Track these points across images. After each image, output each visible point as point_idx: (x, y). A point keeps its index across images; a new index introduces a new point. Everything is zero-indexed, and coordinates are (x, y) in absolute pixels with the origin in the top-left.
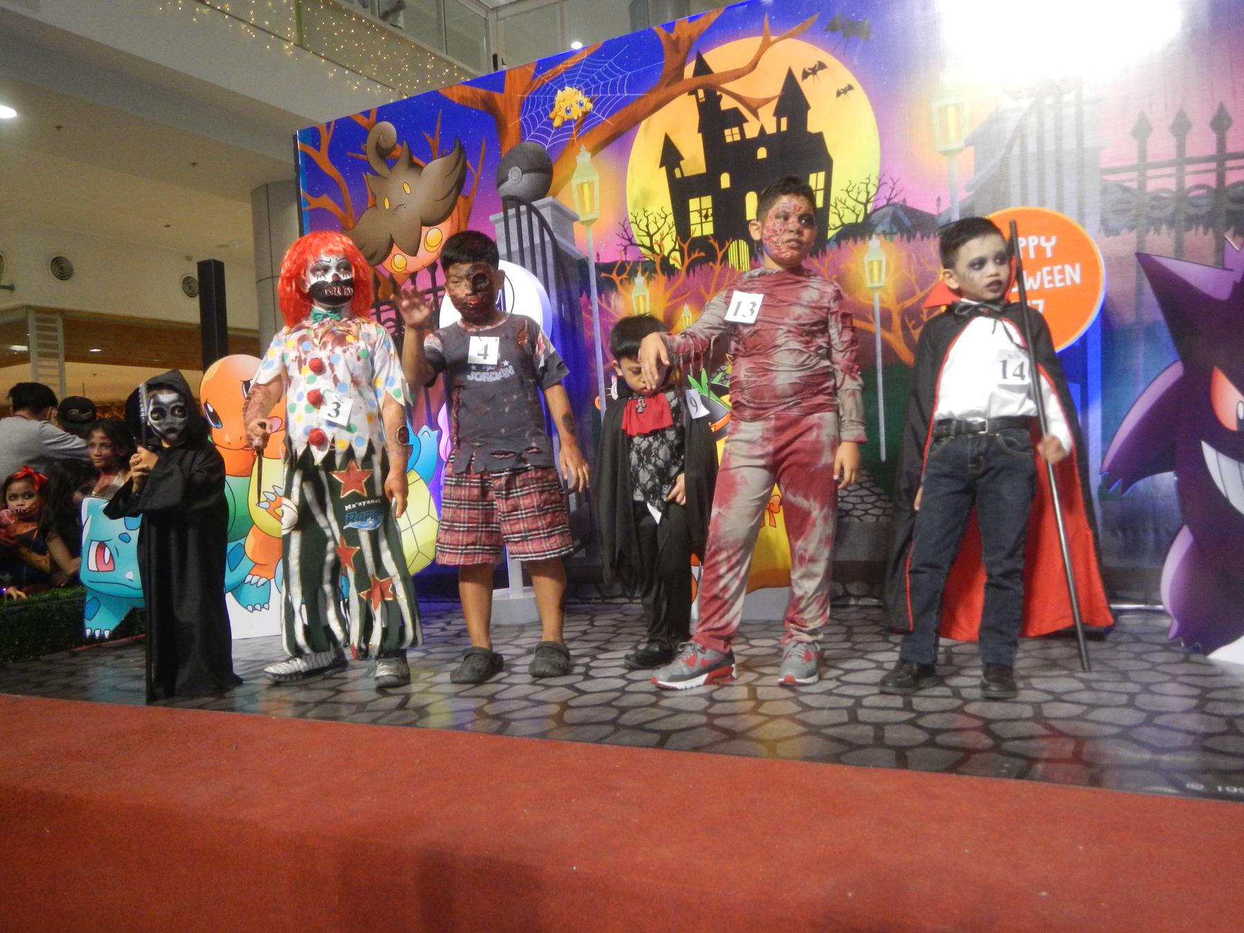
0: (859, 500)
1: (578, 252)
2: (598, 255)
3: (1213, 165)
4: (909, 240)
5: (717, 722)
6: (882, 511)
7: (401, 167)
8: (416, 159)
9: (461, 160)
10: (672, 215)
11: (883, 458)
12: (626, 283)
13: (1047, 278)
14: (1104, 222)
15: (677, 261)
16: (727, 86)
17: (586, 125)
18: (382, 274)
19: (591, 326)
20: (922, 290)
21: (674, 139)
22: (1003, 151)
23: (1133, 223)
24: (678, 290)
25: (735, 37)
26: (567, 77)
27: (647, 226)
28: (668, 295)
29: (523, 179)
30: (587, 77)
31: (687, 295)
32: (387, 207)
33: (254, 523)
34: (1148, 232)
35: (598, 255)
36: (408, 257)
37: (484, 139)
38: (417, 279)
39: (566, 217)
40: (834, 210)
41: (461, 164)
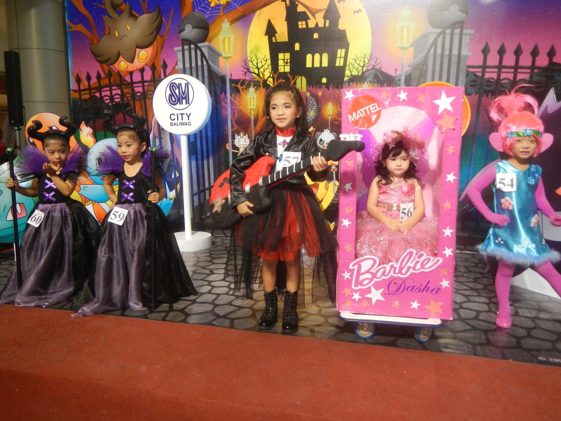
1: (221, 72)
2: (231, 75)
7: (125, 15)
8: (134, 12)
9: (159, 17)
12: (245, 90)
14: (466, 89)
15: (271, 83)
17: (228, 9)
19: (226, 109)
22: (426, 51)
23: (478, 91)
27: (257, 64)
29: (193, 31)
32: (117, 35)
34: (483, 96)
35: (231, 75)
36: (127, 62)
37: (172, 9)
38: (134, 75)
39: (215, 54)
41: (159, 19)
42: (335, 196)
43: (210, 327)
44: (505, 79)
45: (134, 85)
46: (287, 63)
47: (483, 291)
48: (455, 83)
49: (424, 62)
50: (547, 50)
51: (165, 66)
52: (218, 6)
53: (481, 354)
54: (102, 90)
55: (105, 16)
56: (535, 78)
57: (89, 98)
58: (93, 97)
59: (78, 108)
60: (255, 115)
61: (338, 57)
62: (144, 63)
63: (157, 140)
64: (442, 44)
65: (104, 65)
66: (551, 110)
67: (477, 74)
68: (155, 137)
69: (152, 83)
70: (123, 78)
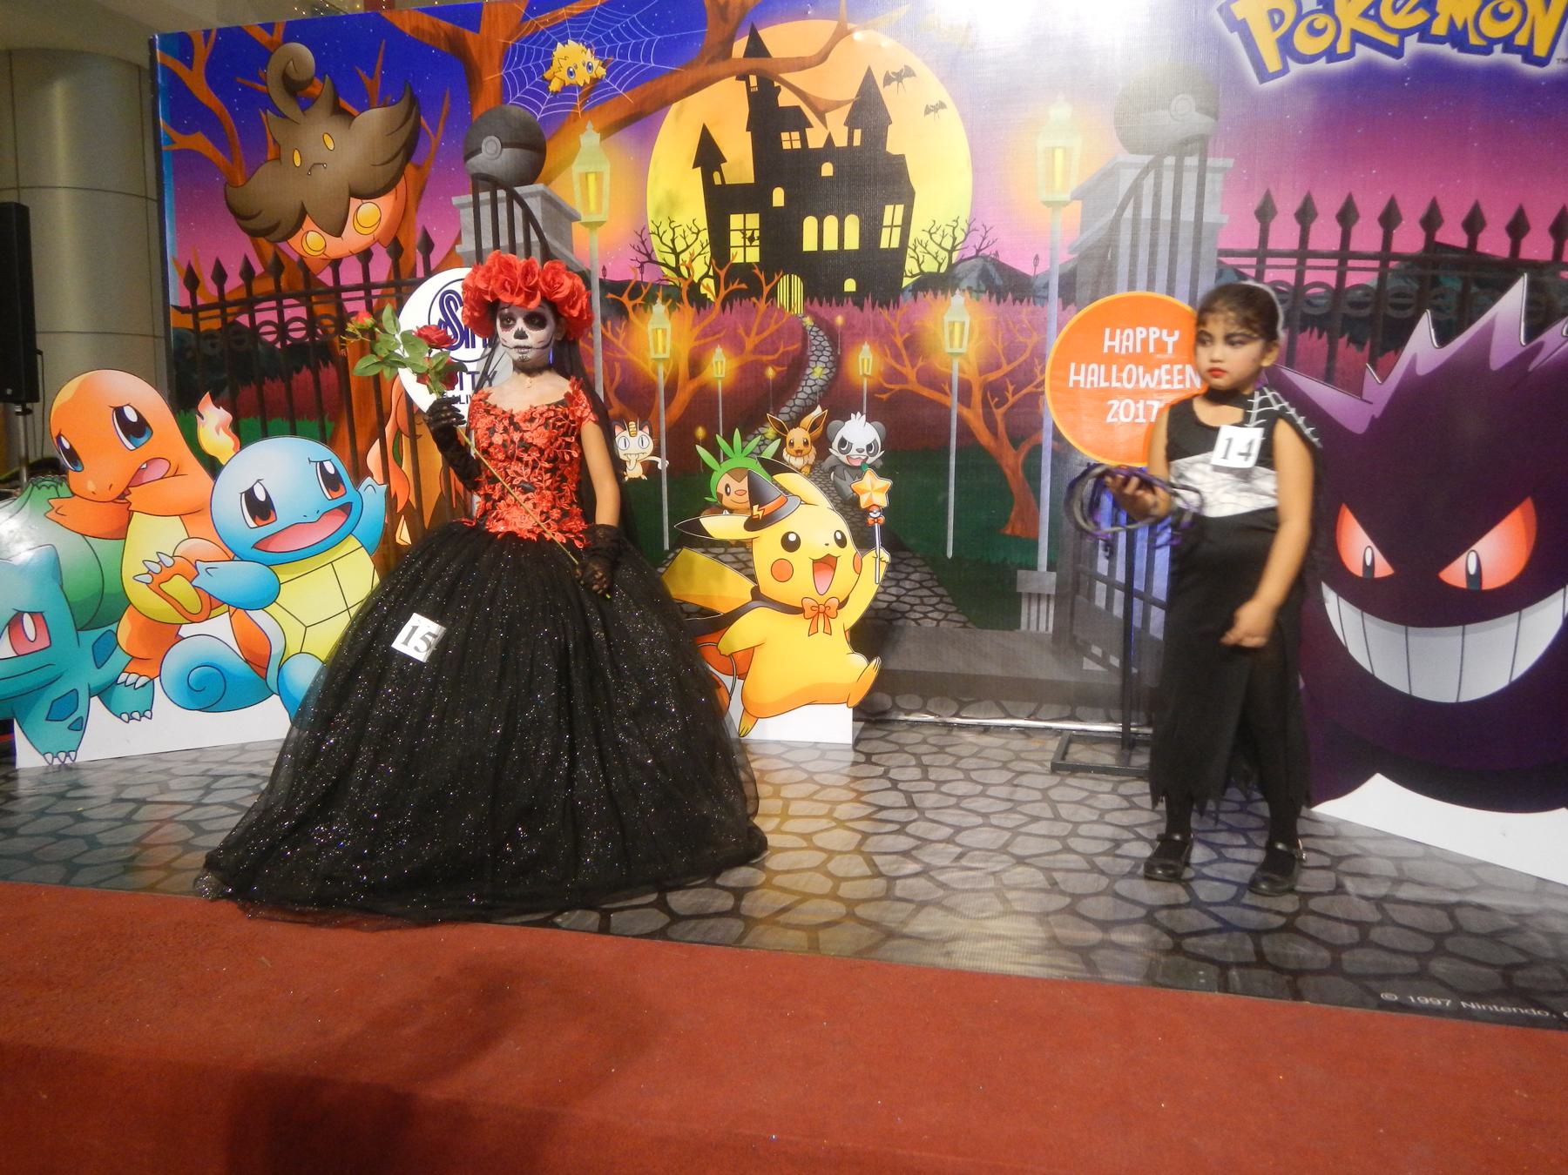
0: (918, 601)
1: (574, 260)
2: (604, 269)
3: (1334, 262)
4: (998, 302)
5: (861, 911)
6: (943, 615)
7: (320, 111)
8: (343, 103)
10: (706, 232)
11: (950, 554)
13: (1165, 377)
16: (788, 77)
17: (595, 97)
18: (289, 257)
19: (592, 364)
20: (1008, 363)
21: (715, 133)
22: (1114, 211)
24: (710, 325)
25: (804, 16)
26: (571, 28)
27: (673, 241)
28: (697, 331)
29: (503, 155)
30: (601, 32)
31: (722, 334)
32: (298, 163)
33: (131, 603)
35: (604, 269)
36: (327, 237)
37: (447, 96)
38: (340, 268)
39: (563, 215)
40: (913, 254)
41: (411, 121)
42: (881, 590)
43: (548, 931)
44: (1315, 285)
45: (344, 295)
46: (752, 239)
47: (1258, 833)
48: (1188, 294)
49: (1109, 243)
50: (1422, 211)
51: (427, 245)
52: (568, 89)
53: (1238, 986)
54: (256, 308)
55: (266, 113)
56: (1393, 284)
57: (220, 329)
58: (230, 327)
59: (189, 355)
60: (668, 374)
61: (884, 224)
62: (369, 239)
63: (406, 442)
64: (1152, 193)
65: (262, 241)
66: (1422, 369)
67: (1245, 271)
68: (398, 433)
69: (393, 290)
70: (314, 275)
